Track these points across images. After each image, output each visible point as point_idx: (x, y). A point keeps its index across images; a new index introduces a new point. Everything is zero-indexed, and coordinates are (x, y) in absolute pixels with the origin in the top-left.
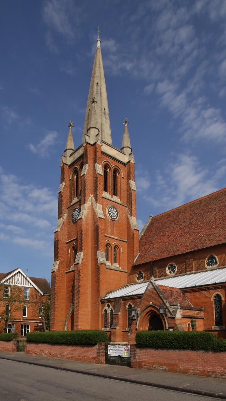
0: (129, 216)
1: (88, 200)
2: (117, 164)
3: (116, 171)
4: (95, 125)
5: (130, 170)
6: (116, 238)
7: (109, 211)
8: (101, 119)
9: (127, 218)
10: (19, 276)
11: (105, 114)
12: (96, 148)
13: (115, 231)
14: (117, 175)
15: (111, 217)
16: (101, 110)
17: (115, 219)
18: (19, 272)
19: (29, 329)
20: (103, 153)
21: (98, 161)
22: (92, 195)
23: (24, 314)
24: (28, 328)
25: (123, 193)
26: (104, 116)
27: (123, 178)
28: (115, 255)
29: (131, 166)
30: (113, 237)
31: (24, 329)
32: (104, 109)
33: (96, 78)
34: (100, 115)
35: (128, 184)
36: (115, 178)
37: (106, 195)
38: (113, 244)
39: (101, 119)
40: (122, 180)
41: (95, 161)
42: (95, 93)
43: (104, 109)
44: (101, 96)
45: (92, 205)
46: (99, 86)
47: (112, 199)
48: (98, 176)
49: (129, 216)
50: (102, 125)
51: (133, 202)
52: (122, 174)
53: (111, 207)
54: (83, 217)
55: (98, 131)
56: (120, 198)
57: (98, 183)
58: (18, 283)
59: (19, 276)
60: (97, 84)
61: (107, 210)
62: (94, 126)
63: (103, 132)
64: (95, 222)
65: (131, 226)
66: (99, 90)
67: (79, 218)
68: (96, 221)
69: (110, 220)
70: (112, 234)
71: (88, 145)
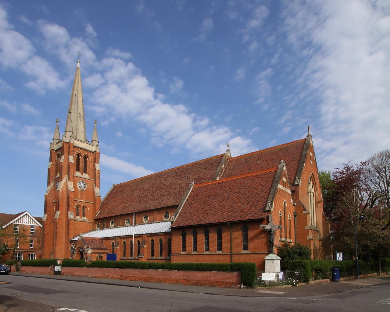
0: (94, 186)
1: (64, 179)
2: (86, 153)
3: (86, 157)
4: (70, 129)
5: (96, 157)
6: (85, 201)
7: (79, 185)
8: (77, 121)
9: (93, 188)
10: (27, 217)
11: (80, 118)
12: (69, 145)
13: (83, 197)
14: (87, 159)
15: (81, 188)
16: (77, 115)
17: (84, 189)
18: (27, 214)
19: (35, 257)
20: (74, 147)
21: (70, 154)
22: (67, 176)
23: (31, 246)
24: (34, 256)
25: (91, 172)
26: (79, 119)
27: (91, 161)
28: (83, 212)
29: (97, 154)
30: (82, 201)
31: (31, 257)
32: (80, 114)
33: (75, 91)
34: (76, 118)
35: (94, 165)
36: (85, 162)
37: (78, 174)
38: (82, 205)
39: (77, 121)
40: (90, 163)
41: (69, 154)
42: (74, 102)
43: (80, 114)
44: (78, 105)
45: (66, 182)
46: (77, 97)
47: (82, 176)
48: (70, 164)
49: (94, 186)
50: (77, 125)
51: (97, 178)
52: (91, 159)
53: (81, 182)
54: (60, 190)
55: (72, 133)
56: (88, 175)
57: (70, 168)
58: (26, 223)
59: (27, 217)
60: (76, 95)
61: (78, 184)
62: (69, 130)
63: (78, 131)
64: (68, 193)
65: (95, 193)
66: (77, 100)
67: (58, 190)
68: (68, 192)
69: (80, 190)
70: (82, 199)
71: (65, 143)
